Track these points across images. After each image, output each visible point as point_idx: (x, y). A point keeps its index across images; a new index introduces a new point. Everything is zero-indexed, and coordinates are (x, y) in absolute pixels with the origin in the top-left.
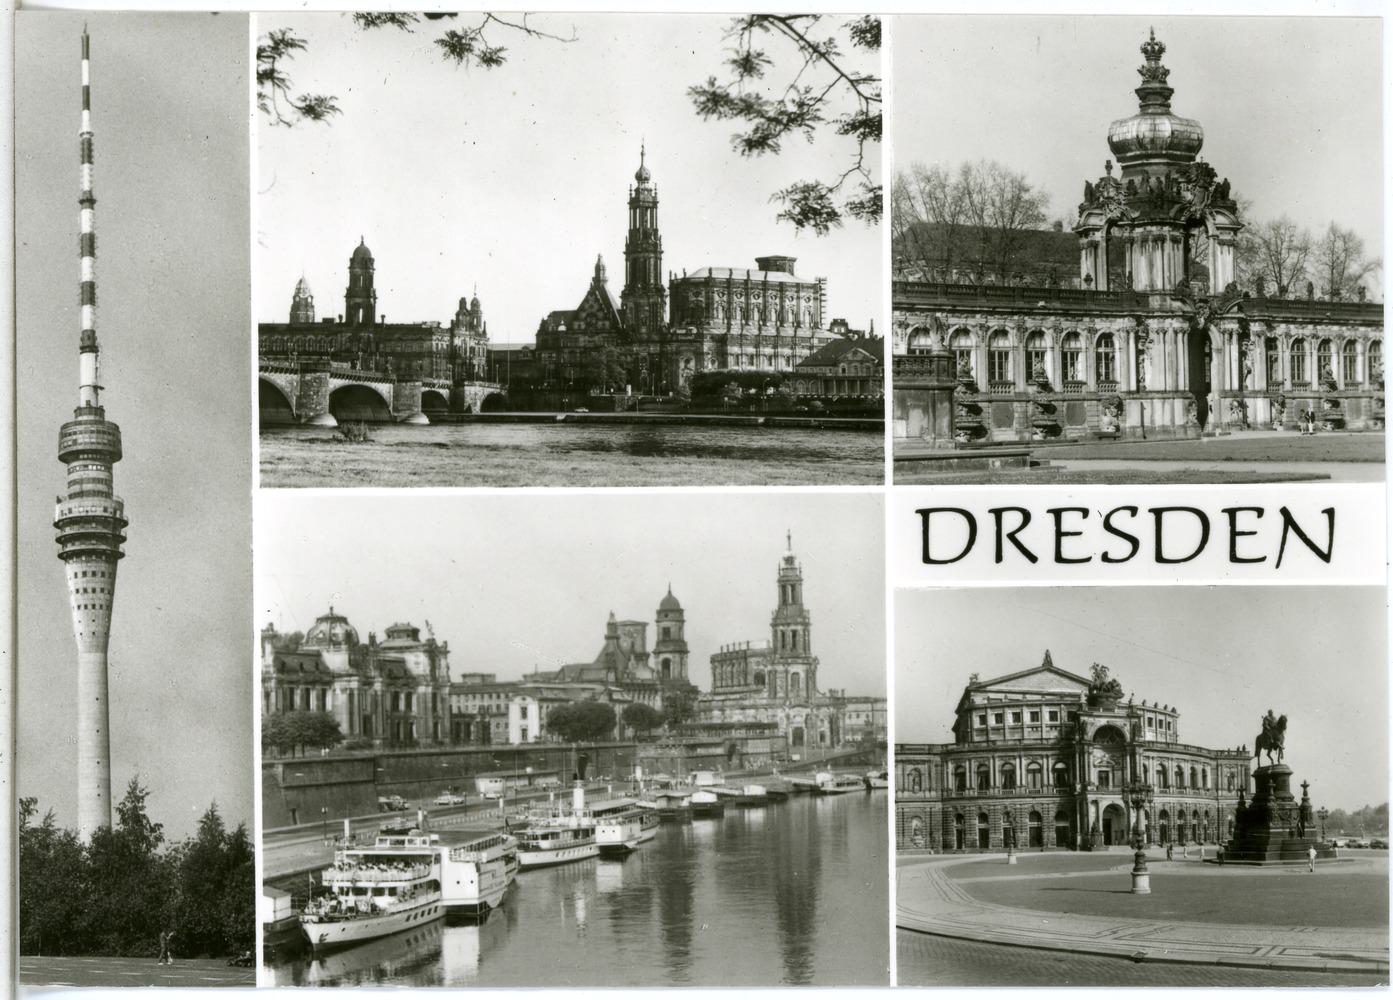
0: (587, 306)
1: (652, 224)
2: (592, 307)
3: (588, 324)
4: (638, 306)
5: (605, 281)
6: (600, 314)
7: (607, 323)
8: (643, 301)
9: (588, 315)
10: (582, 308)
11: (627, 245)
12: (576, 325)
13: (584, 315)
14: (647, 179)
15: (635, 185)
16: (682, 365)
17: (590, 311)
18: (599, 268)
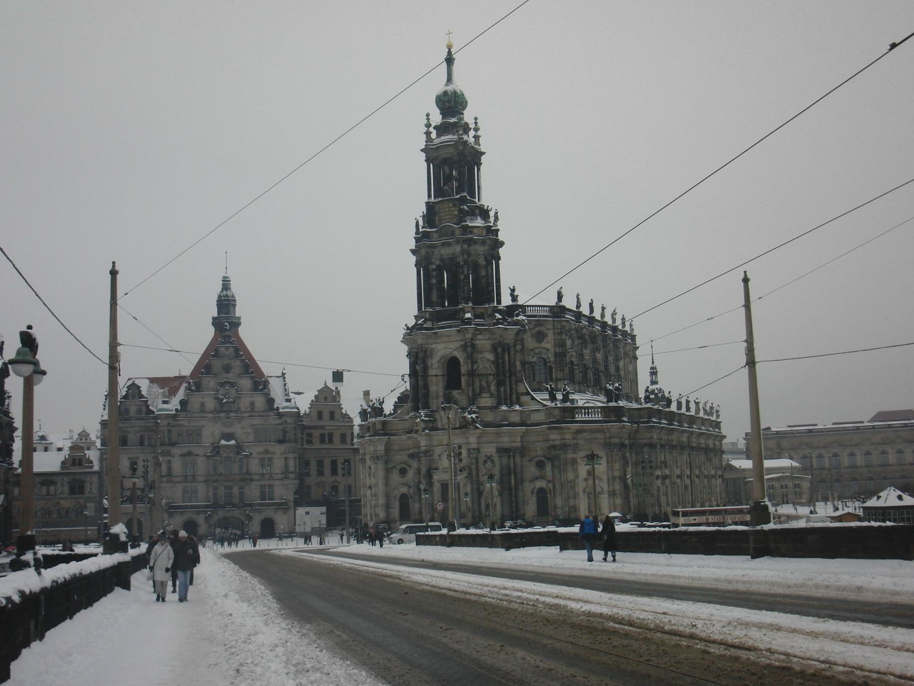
0: (217, 364)
2: (227, 369)
4: (473, 346)
5: (236, 324)
15: (437, 118)
16: (583, 469)
17: (224, 377)
18: (226, 304)
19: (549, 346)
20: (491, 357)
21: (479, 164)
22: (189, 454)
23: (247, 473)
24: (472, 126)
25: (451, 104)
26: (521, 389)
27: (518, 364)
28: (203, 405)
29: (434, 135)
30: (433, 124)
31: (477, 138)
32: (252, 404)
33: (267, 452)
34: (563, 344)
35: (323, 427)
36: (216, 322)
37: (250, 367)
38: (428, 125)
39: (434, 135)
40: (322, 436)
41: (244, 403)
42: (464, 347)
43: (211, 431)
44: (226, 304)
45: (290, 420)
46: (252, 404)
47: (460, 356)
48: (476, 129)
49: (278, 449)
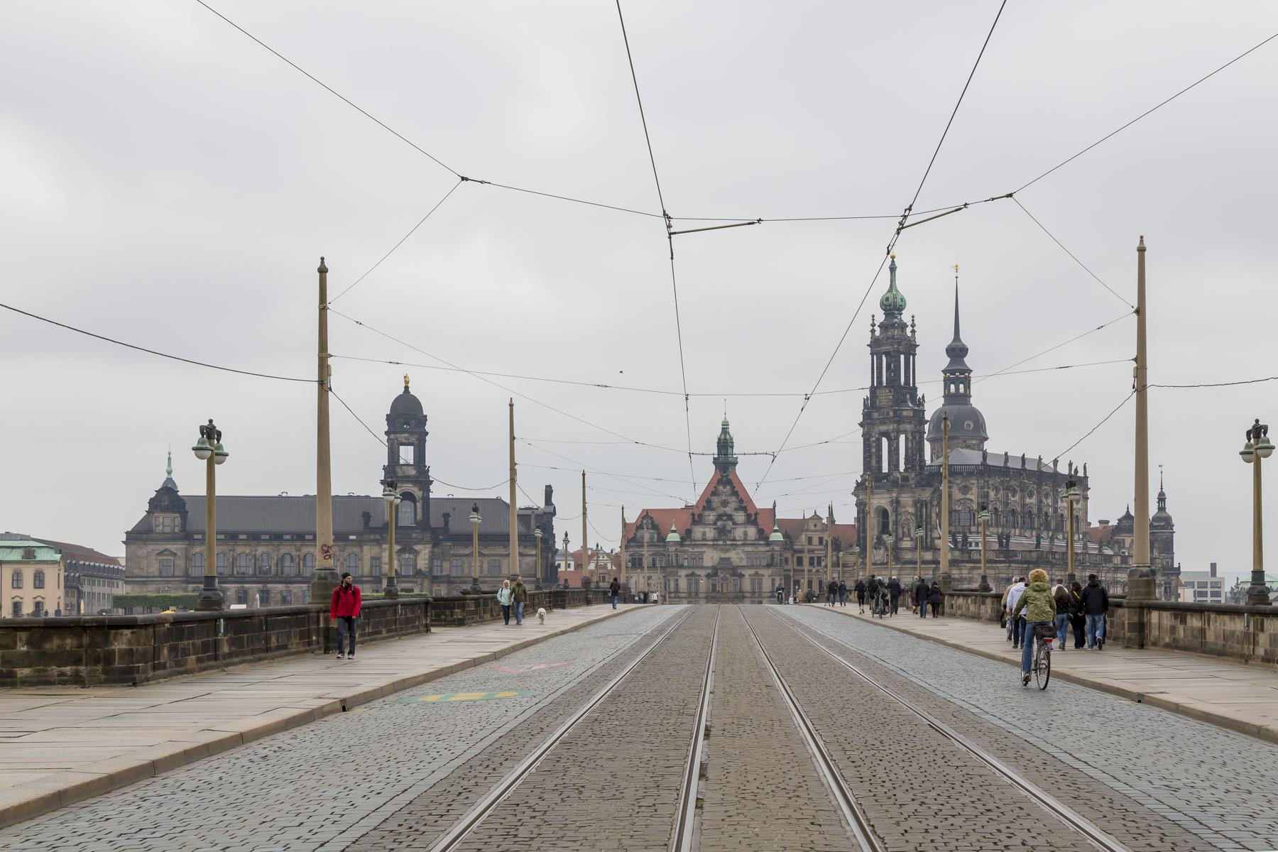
0: (716, 501)
1: (907, 378)
2: (725, 504)
3: (722, 532)
4: (898, 502)
6: (740, 517)
7: (752, 531)
8: (907, 499)
9: (720, 517)
10: (706, 503)
11: (867, 415)
12: (698, 532)
13: (711, 516)
14: (900, 309)
15: (880, 317)
17: (722, 510)
18: (725, 444)
19: (972, 497)
20: (911, 510)
21: (914, 355)
22: (693, 574)
23: (741, 591)
24: (909, 323)
25: (892, 307)
26: (935, 535)
27: (934, 515)
28: (704, 533)
29: (877, 333)
30: (877, 323)
31: (913, 332)
32: (745, 533)
33: (757, 573)
34: (987, 496)
35: (812, 551)
36: (716, 461)
37: (743, 503)
38: (873, 325)
39: (877, 333)
40: (812, 559)
41: (739, 533)
42: (892, 502)
43: (711, 557)
44: (725, 444)
45: (777, 548)
46: (745, 533)
47: (889, 509)
48: (913, 326)
49: (767, 572)
